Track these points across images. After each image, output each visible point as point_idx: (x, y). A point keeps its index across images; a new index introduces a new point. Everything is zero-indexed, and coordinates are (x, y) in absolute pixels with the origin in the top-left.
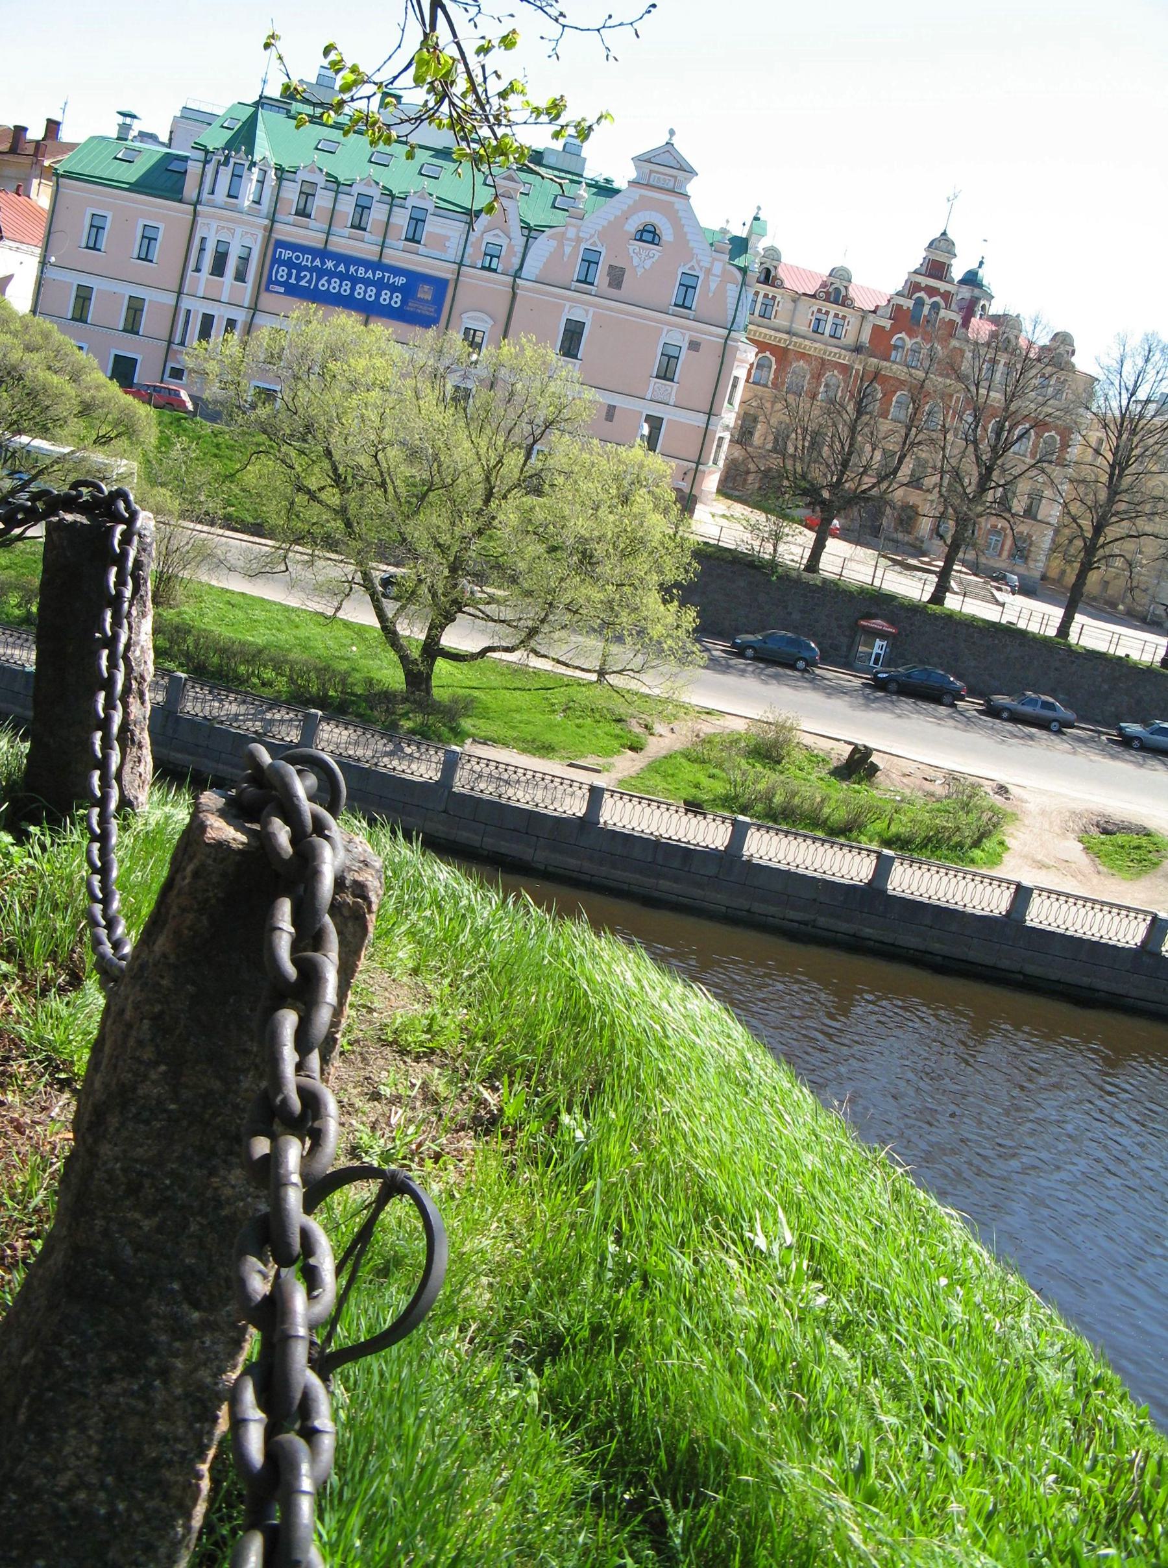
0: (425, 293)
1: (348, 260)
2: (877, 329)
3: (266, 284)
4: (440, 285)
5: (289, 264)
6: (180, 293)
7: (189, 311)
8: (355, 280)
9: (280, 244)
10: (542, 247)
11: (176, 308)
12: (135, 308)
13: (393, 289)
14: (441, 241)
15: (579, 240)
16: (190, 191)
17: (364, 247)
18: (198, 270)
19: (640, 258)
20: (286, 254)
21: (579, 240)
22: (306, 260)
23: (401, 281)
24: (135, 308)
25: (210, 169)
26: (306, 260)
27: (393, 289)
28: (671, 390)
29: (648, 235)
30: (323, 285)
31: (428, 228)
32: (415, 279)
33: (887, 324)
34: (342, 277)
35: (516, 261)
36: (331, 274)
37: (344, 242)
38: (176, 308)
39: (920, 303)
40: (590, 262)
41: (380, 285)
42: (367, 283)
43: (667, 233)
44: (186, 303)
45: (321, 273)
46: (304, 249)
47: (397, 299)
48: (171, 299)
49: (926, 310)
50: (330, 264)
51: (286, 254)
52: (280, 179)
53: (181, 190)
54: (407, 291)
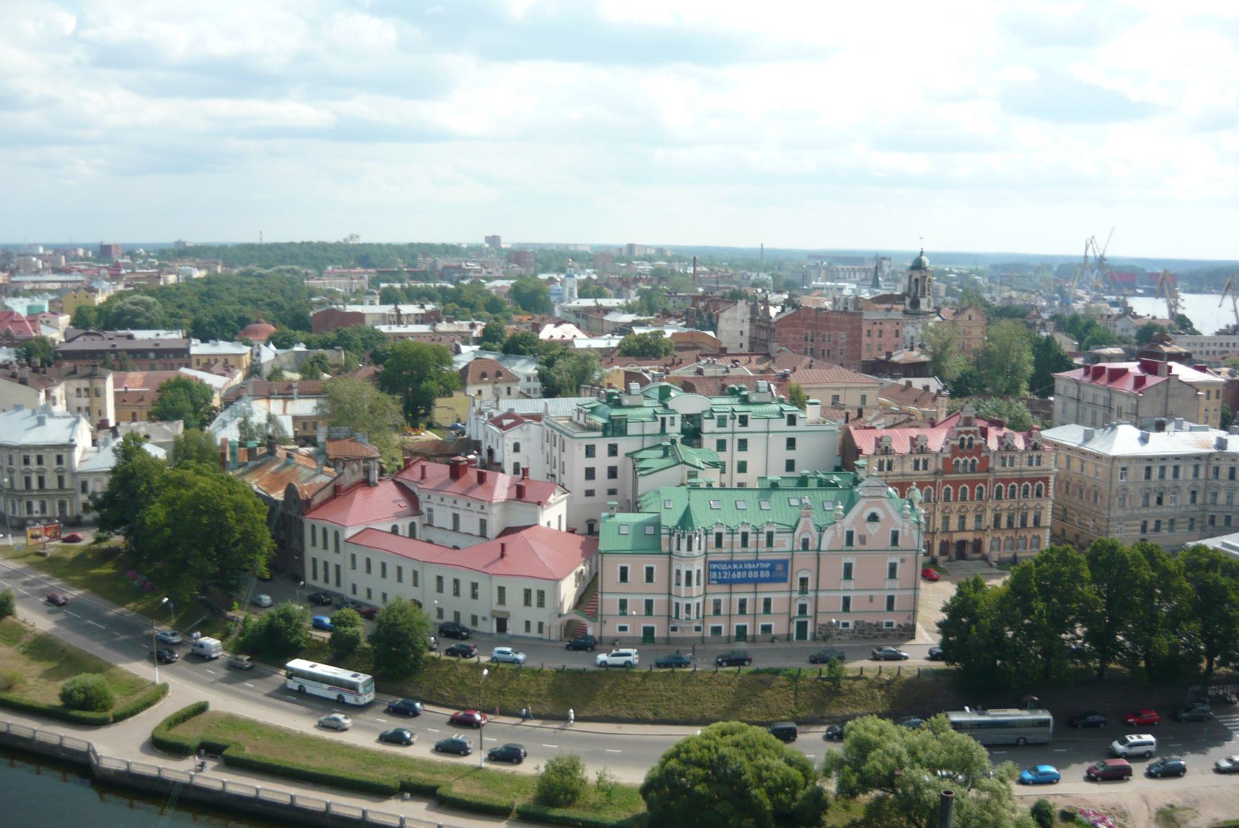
0: (779, 567)
1: (743, 562)
2: (945, 460)
3: (708, 581)
4: (785, 563)
5: (717, 570)
6: (670, 594)
7: (677, 605)
8: (747, 570)
9: (711, 562)
10: (828, 535)
11: (669, 602)
12: (649, 604)
13: (765, 570)
14: (782, 544)
15: (843, 528)
16: (665, 548)
17: (748, 554)
18: (678, 584)
19: (872, 529)
20: (715, 566)
21: (843, 528)
22: (724, 567)
23: (768, 565)
24: (649, 604)
25: (675, 539)
26: (724, 567)
27: (765, 570)
28: (896, 584)
29: (873, 518)
30: (734, 575)
31: (775, 539)
32: (774, 563)
33: (949, 456)
34: (741, 570)
35: (817, 543)
36: (736, 570)
37: (741, 555)
38: (669, 602)
39: (963, 439)
40: (850, 535)
41: (759, 570)
42: (753, 570)
43: (881, 515)
44: (674, 600)
45: (732, 571)
46: (722, 562)
47: (768, 573)
48: (665, 598)
49: (966, 443)
50: (735, 566)
51: (715, 566)
52: (706, 534)
53: (660, 548)
54: (772, 569)
